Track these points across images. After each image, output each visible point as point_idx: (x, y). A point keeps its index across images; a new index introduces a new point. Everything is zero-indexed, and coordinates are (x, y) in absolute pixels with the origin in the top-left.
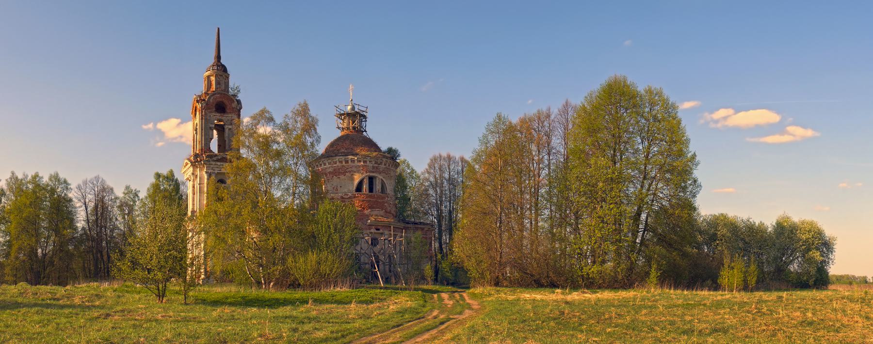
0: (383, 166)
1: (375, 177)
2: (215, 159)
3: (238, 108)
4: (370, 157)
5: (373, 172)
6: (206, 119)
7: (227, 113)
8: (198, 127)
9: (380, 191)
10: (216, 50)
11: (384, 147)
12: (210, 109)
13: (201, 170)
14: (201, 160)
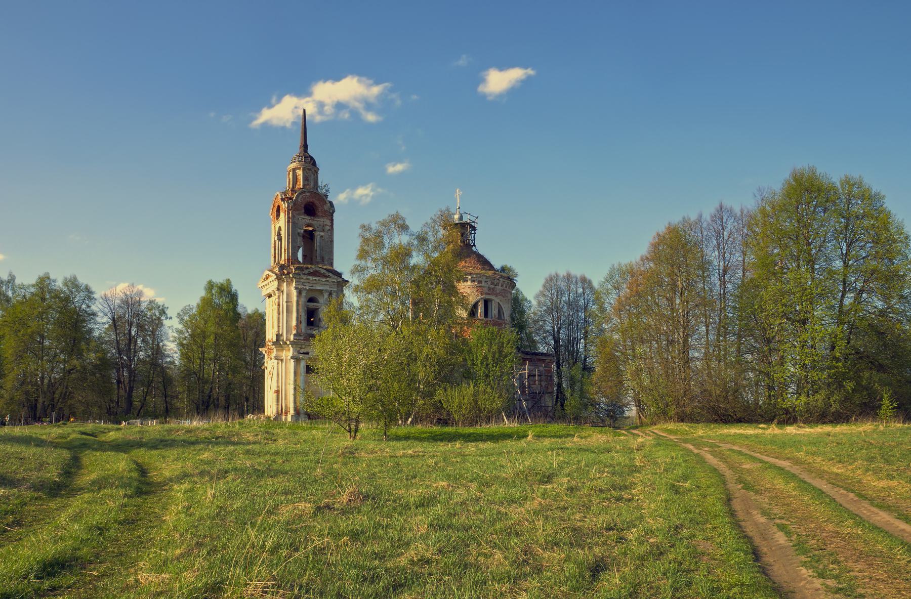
0: (499, 287)
1: (491, 300)
2: (306, 272)
3: (331, 211)
5: (489, 294)
6: (293, 223)
7: (318, 216)
8: (283, 233)
9: (497, 316)
10: (302, 136)
11: (497, 265)
12: (298, 210)
13: (289, 285)
14: (288, 273)
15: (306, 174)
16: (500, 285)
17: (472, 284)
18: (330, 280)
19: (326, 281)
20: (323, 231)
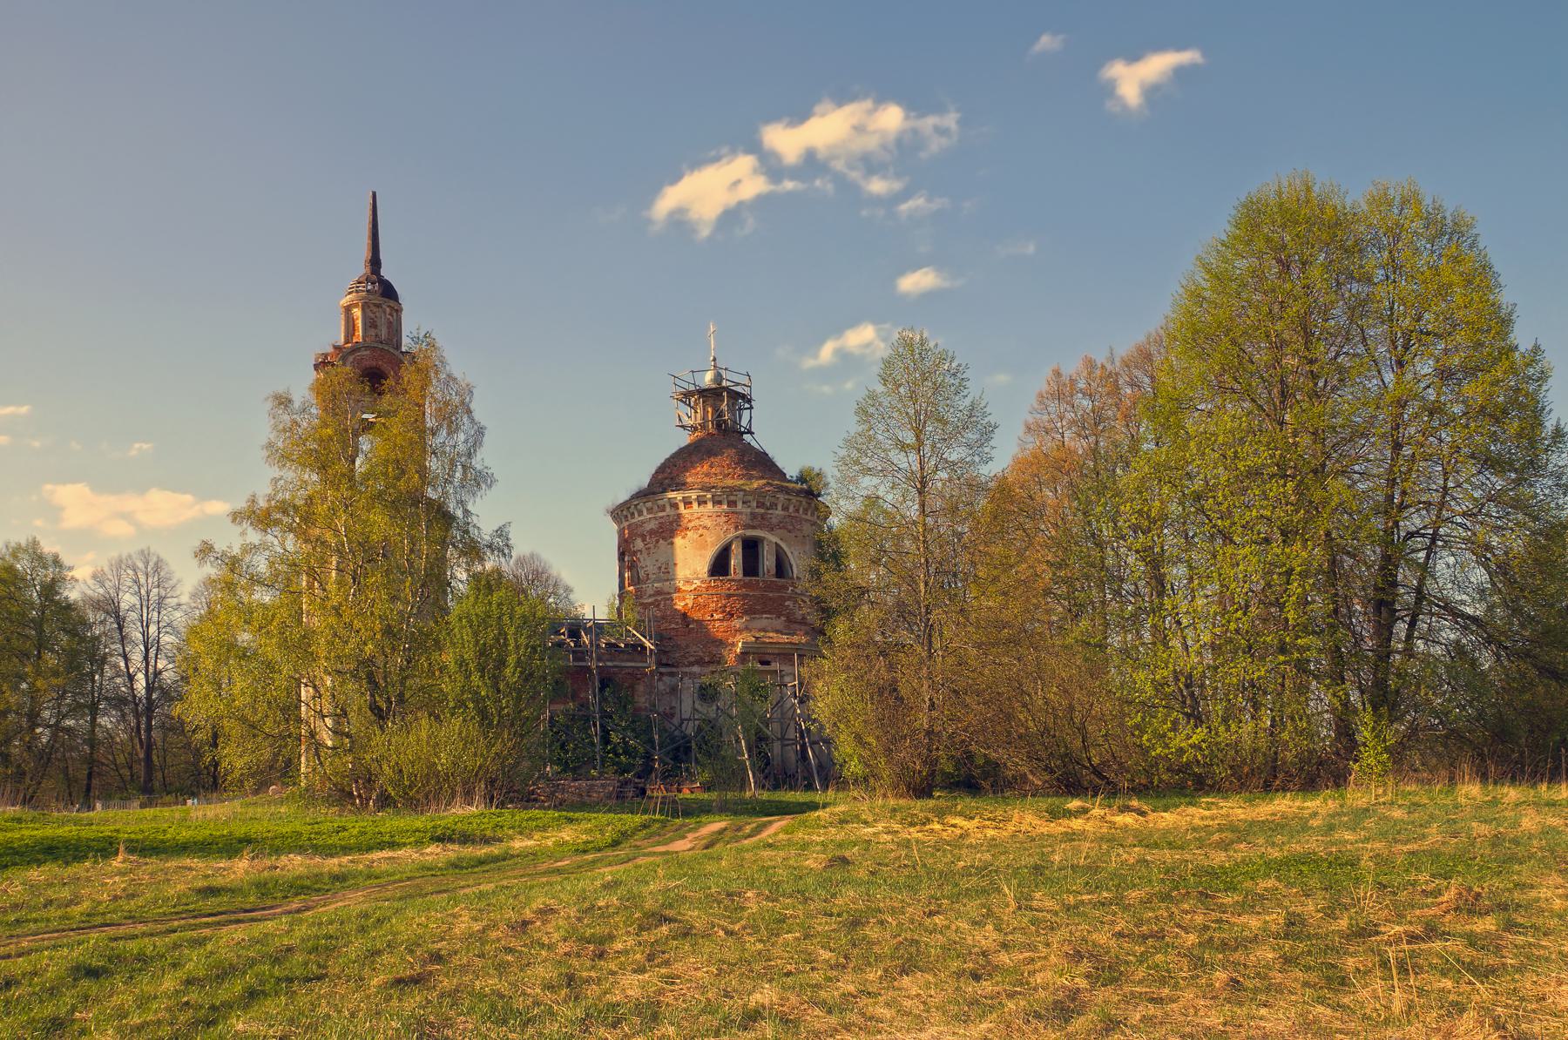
0: (779, 512)
4: (745, 490)
5: (754, 527)
9: (773, 571)
15: (373, 316)
16: (780, 507)
17: (717, 508)
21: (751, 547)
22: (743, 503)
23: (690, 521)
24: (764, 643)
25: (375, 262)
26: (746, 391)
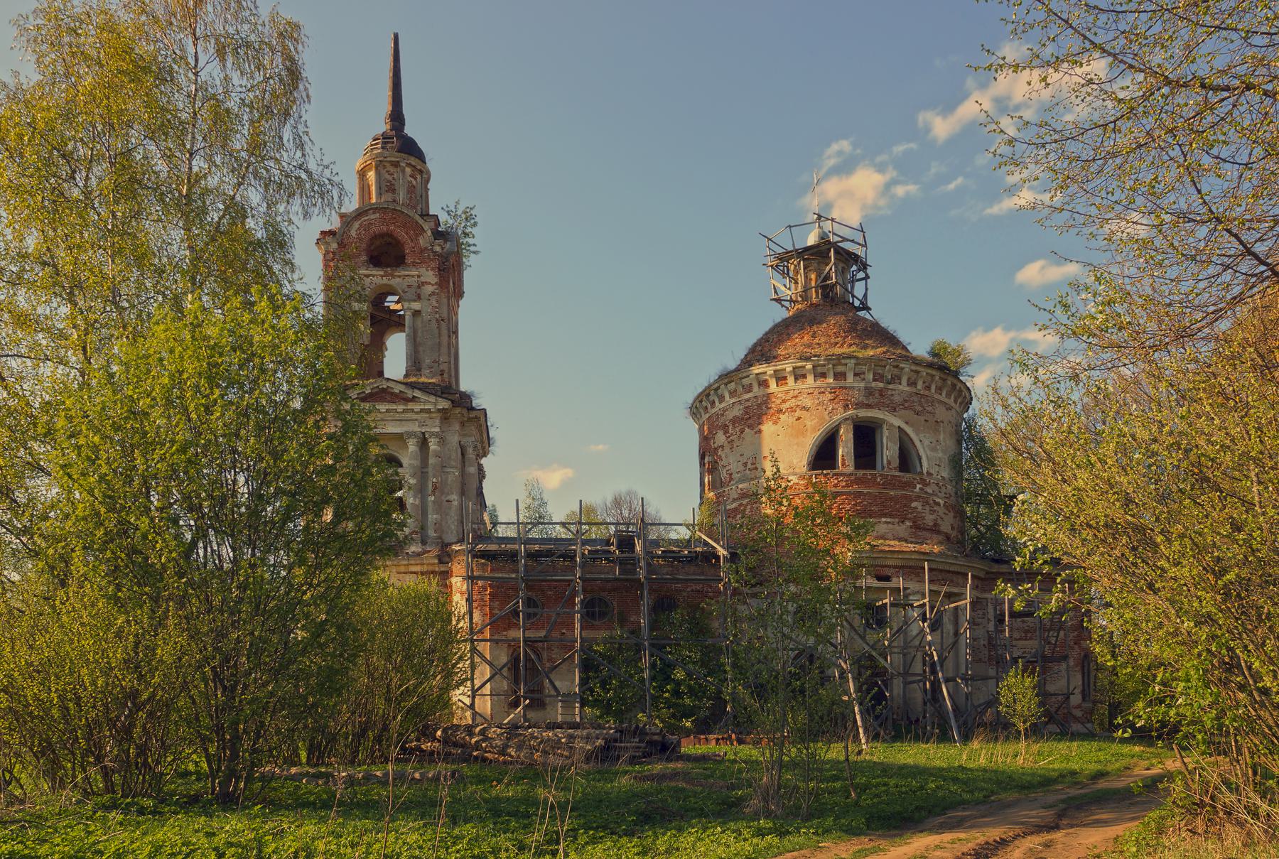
0: (904, 387)
5: (869, 406)
9: (896, 463)
15: (390, 178)
16: (904, 381)
17: (820, 383)
18: (417, 407)
19: (404, 411)
20: (419, 298)
21: (866, 436)
22: (855, 375)
23: (784, 401)
24: (882, 551)
25: (397, 117)
26: (859, 251)
